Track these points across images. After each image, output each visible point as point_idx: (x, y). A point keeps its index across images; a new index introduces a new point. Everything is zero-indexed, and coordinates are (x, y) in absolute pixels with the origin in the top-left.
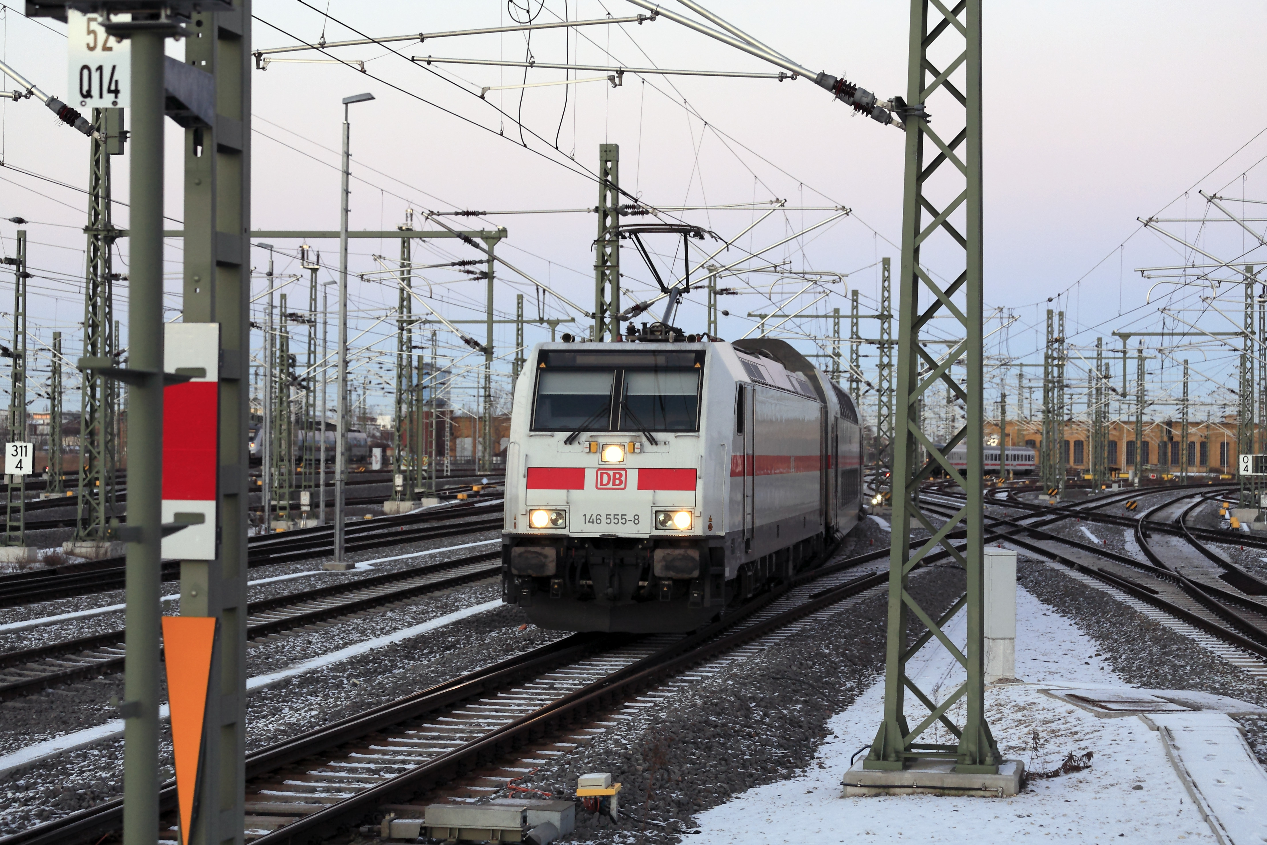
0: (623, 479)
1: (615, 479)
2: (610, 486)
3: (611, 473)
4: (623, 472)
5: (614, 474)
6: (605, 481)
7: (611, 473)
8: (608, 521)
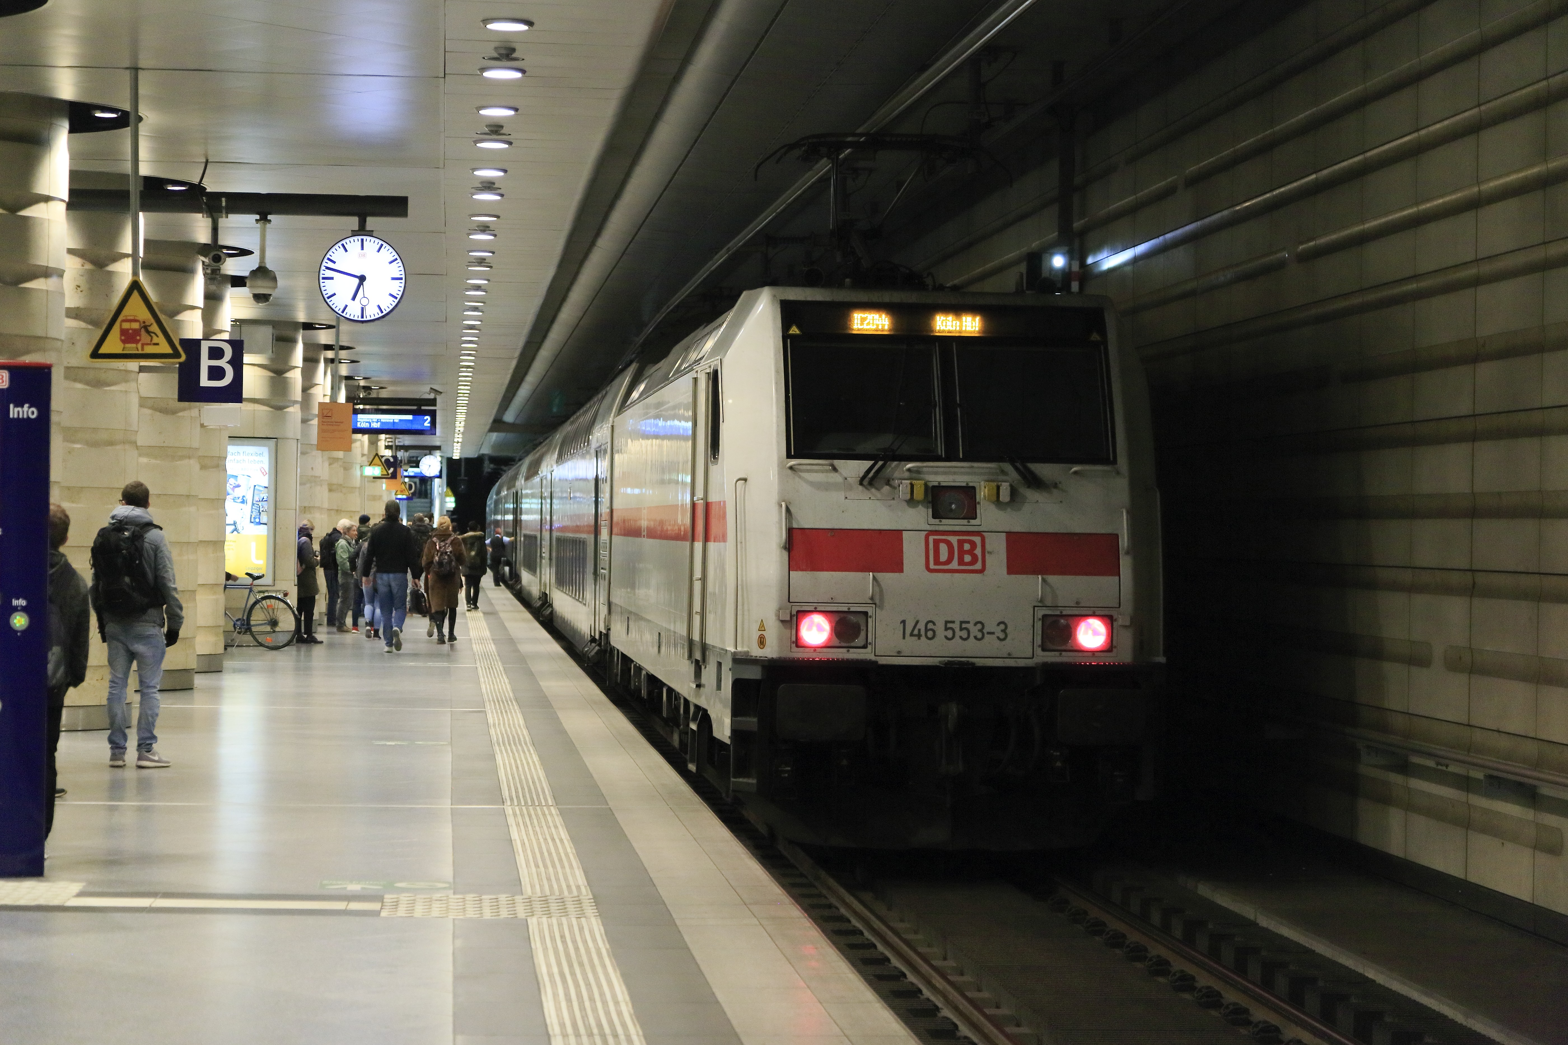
0: (978, 551)
1: (962, 552)
2: (954, 565)
3: (954, 540)
4: (977, 540)
5: (961, 543)
6: (944, 556)
7: (954, 540)
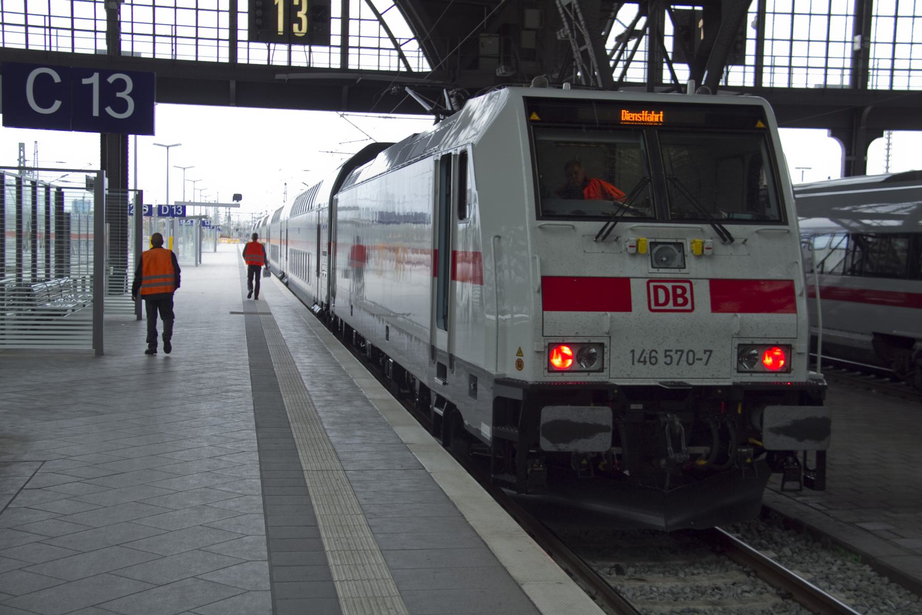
0: (688, 295)
1: (676, 296)
2: (670, 306)
3: (669, 286)
4: (687, 285)
5: (674, 288)
6: (662, 299)
7: (669, 286)
8: (668, 360)
